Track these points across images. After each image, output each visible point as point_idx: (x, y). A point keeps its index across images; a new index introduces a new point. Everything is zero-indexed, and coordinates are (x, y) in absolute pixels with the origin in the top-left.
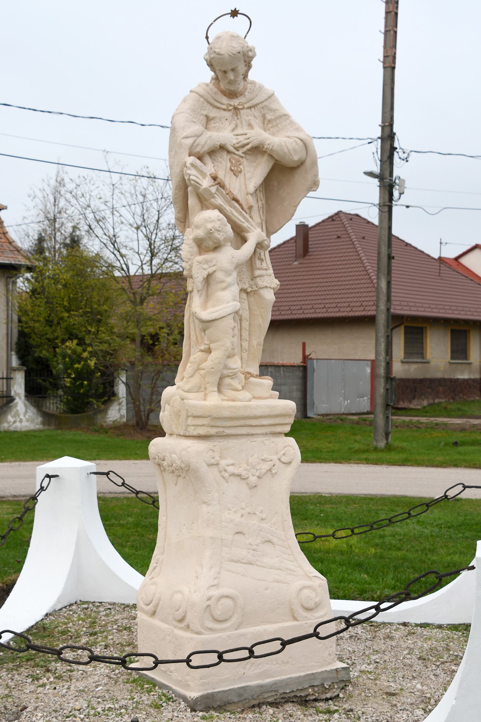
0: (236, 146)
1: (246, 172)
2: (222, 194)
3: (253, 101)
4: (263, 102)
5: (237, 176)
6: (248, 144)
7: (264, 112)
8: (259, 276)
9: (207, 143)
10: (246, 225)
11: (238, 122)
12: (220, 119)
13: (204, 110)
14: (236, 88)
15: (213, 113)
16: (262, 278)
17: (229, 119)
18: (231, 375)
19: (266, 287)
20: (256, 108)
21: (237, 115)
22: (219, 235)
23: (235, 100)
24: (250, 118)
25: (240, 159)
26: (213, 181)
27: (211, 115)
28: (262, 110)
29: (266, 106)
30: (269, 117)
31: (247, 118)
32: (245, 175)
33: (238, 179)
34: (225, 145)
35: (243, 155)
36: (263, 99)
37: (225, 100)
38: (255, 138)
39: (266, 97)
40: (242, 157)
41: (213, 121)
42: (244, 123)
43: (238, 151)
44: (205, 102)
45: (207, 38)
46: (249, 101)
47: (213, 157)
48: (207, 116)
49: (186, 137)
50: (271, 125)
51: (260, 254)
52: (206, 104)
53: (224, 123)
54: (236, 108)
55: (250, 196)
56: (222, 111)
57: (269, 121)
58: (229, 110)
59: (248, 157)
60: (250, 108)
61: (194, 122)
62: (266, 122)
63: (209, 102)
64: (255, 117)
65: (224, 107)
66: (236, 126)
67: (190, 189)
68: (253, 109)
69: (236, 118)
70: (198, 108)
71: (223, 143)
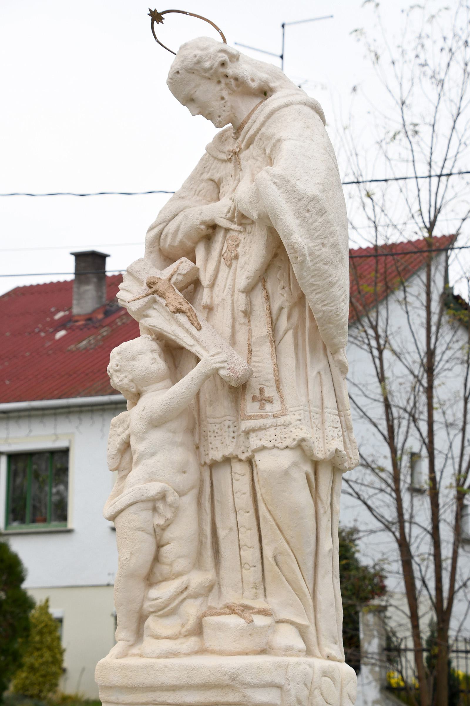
8: (254, 430)
9: (181, 226)
10: (196, 349)
16: (261, 434)
18: (152, 610)
19: (263, 448)
22: (118, 377)
27: (216, 177)
44: (211, 158)
51: (261, 390)
61: (183, 198)
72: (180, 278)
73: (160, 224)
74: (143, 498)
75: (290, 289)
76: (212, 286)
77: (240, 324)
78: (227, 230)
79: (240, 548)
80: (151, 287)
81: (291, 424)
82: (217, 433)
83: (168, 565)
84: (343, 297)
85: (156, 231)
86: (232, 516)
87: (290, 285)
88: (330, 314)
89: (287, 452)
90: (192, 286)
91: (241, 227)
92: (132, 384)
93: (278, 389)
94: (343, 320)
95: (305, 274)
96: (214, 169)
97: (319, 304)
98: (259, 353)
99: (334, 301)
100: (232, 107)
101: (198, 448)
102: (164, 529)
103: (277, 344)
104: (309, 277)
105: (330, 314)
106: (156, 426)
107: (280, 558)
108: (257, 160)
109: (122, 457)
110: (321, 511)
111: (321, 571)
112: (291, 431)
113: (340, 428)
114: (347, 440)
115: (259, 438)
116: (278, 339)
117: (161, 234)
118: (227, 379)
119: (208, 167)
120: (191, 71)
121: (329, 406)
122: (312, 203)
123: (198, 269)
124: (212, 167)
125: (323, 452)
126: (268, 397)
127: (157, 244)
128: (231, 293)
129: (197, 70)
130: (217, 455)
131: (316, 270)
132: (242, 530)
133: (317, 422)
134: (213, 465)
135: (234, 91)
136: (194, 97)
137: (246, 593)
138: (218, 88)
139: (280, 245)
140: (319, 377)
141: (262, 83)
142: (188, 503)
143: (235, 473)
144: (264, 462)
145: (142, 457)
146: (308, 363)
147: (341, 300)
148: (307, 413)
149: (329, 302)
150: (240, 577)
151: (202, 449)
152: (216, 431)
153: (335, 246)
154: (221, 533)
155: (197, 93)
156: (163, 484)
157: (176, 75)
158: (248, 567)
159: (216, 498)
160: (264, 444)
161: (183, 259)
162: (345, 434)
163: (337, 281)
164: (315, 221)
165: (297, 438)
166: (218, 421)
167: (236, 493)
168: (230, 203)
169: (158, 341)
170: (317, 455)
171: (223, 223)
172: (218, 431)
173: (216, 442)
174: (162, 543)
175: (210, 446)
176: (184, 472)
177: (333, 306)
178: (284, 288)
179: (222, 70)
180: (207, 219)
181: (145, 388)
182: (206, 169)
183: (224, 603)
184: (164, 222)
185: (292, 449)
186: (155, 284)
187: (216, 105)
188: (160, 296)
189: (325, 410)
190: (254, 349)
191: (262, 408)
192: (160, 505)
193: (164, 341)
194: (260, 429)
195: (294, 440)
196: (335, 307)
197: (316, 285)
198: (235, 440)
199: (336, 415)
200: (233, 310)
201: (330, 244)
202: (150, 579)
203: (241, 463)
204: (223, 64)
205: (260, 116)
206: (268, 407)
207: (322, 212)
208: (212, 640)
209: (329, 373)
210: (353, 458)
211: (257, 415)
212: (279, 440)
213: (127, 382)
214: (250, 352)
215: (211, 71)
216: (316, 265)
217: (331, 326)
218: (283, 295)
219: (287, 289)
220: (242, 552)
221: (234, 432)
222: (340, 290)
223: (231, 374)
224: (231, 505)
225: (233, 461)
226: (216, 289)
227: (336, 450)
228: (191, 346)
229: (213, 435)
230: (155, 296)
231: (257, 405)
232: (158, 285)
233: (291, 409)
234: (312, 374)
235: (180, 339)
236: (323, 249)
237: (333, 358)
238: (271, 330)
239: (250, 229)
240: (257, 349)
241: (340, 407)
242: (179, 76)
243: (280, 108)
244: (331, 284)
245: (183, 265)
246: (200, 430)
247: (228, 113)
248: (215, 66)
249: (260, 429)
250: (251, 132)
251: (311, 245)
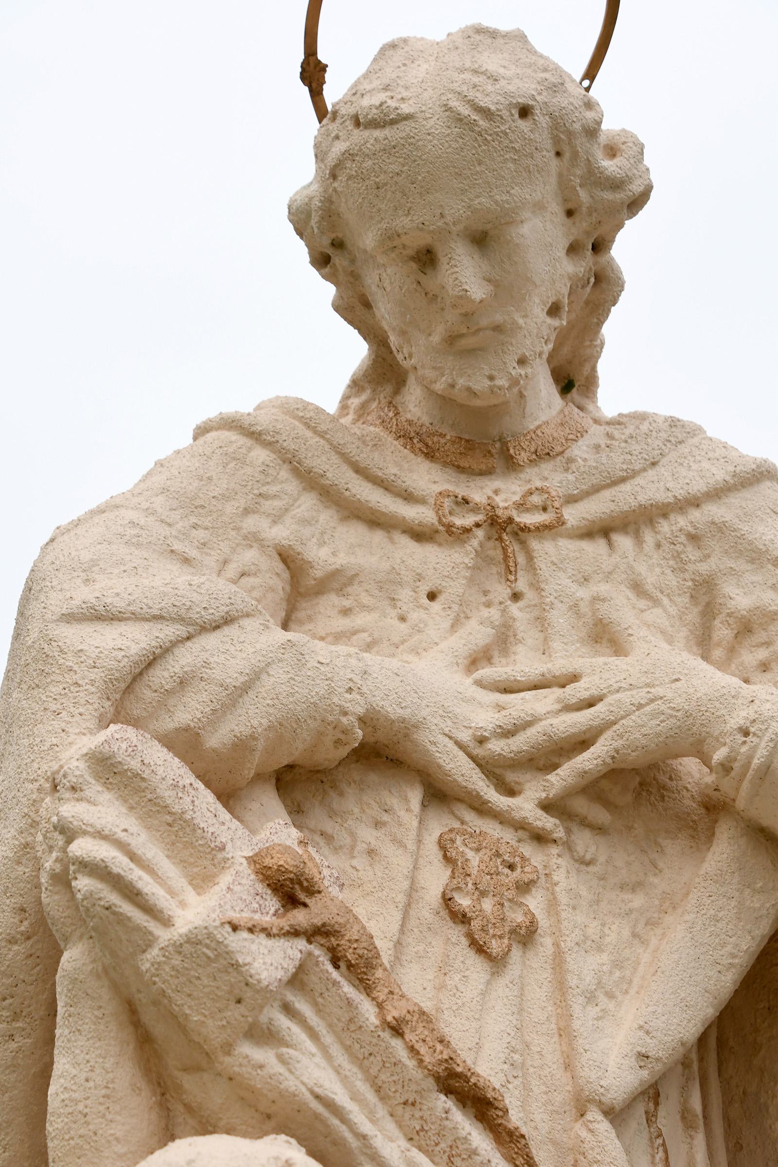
0: (497, 746)
1: (568, 943)
2: (350, 1025)
3: (626, 487)
4: (694, 502)
5: (498, 963)
6: (582, 743)
7: (703, 568)
9: (267, 682)
11: (514, 609)
12: (388, 586)
13: (276, 519)
14: (501, 382)
15: (335, 546)
17: (454, 588)
20: (649, 538)
21: (509, 571)
23: (496, 483)
24: (603, 588)
25: (527, 849)
26: (272, 903)
28: (692, 553)
29: (720, 528)
30: (740, 596)
31: (583, 593)
32: (558, 961)
33: (503, 988)
34: (407, 729)
35: (547, 822)
36: (698, 486)
37: (427, 478)
38: (640, 696)
39: (719, 474)
40: (540, 838)
41: (330, 602)
42: (560, 618)
43: (511, 792)
44: (284, 473)
45: (313, 73)
46: (596, 489)
47: (318, 818)
48: (289, 559)
49: (101, 616)
50: (762, 654)
52: (292, 486)
53: (415, 616)
54: (499, 526)
55: (603, 1126)
56: (405, 541)
57: (745, 628)
58: (449, 528)
59: (584, 841)
60: (602, 531)
62: (722, 632)
63: (312, 481)
64: (638, 588)
65: (420, 514)
66: (504, 640)
67: (73, 958)
68: (624, 542)
69: (501, 591)
70: (225, 498)
71: (392, 710)
73: (158, 618)
96: (305, 522)
108: (656, 602)
119: (277, 503)
129: (575, 155)
182: (267, 505)
184: (181, 620)
188: (335, 962)
215: (608, 196)
242: (524, 125)
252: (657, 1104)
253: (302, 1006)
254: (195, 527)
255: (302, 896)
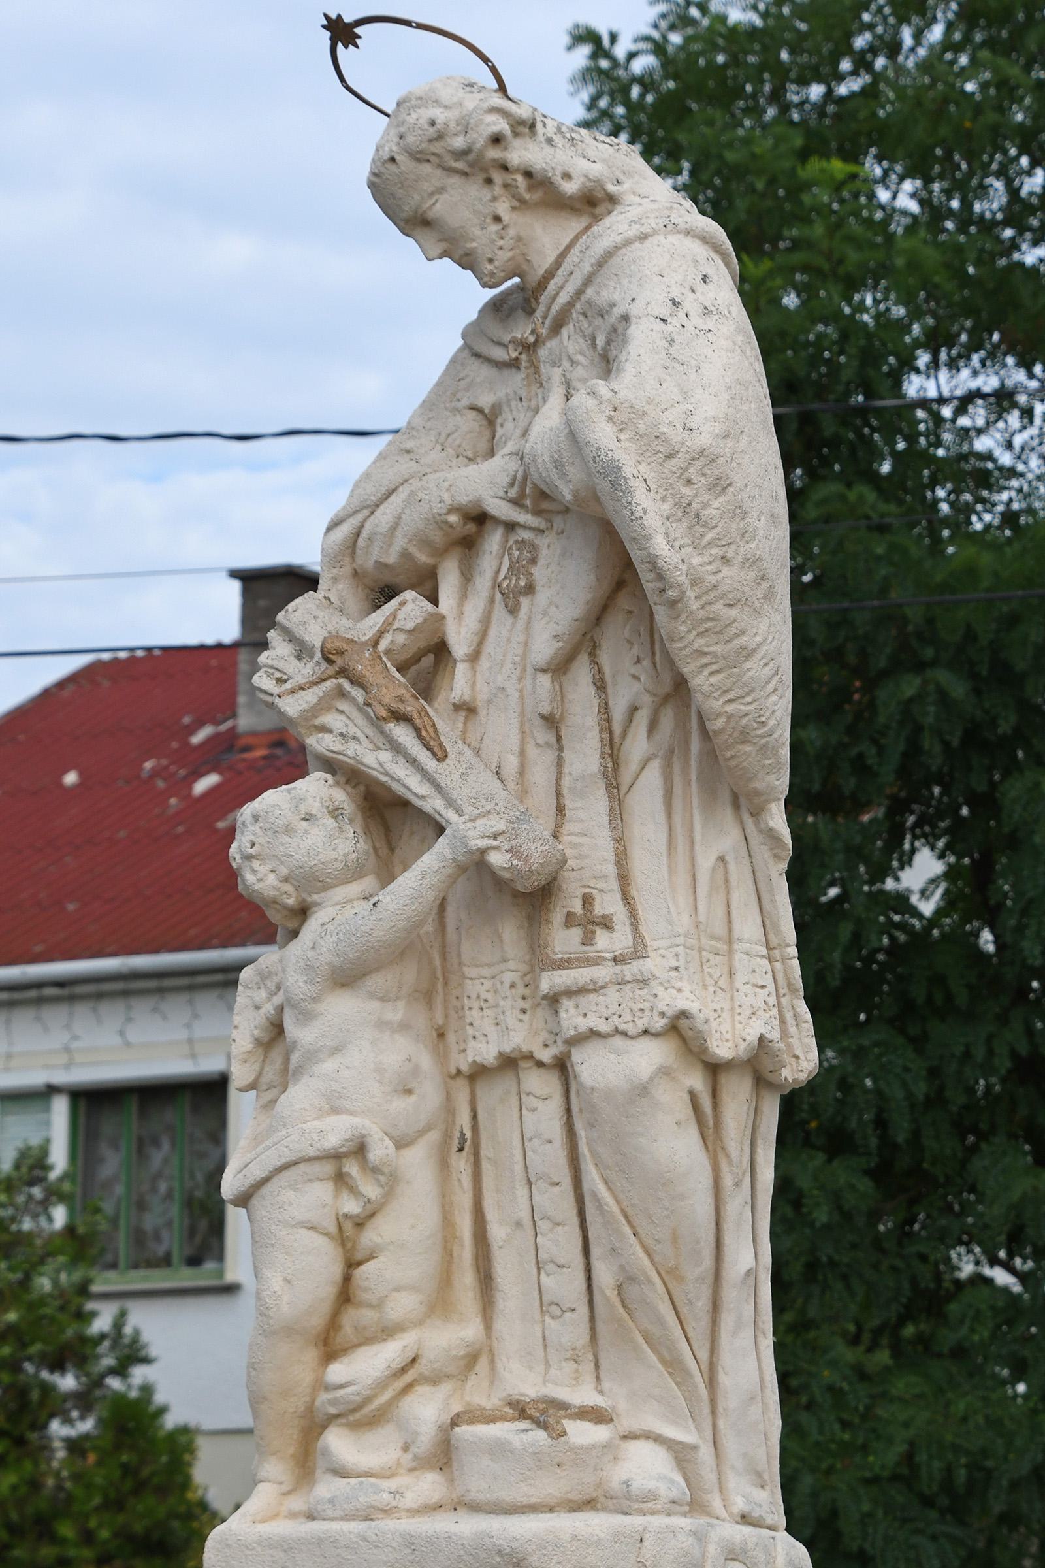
10: (433, 804)
18: (333, 1410)
19: (593, 1034)
22: (254, 871)
27: (486, 400)
51: (587, 900)
72: (401, 638)
73: (356, 512)
74: (312, 1153)
75: (654, 664)
76: (474, 657)
77: (538, 745)
78: (511, 526)
79: (539, 1269)
80: (330, 662)
81: (655, 977)
82: (486, 1000)
83: (370, 1306)
84: (774, 682)
85: (346, 529)
86: (522, 1192)
87: (653, 654)
88: (744, 721)
89: (646, 1044)
90: (430, 659)
91: (540, 520)
92: (288, 888)
93: (627, 898)
94: (775, 736)
95: (683, 628)
97: (716, 699)
98: (582, 815)
99: (752, 691)
100: (519, 239)
101: (441, 1035)
102: (360, 1223)
103: (622, 793)
104: (691, 637)
105: (744, 721)
106: (343, 985)
107: (633, 1291)
109: (266, 1057)
110: (728, 1181)
111: (727, 1321)
112: (656, 995)
113: (771, 988)
114: (789, 1016)
115: (581, 1011)
116: (626, 778)
117: (358, 535)
118: (506, 875)
119: (468, 380)
120: (419, 157)
121: (746, 936)
122: (698, 465)
123: (444, 617)
124: (478, 379)
125: (730, 1044)
126: (604, 917)
127: (347, 559)
128: (518, 672)
130: (486, 1051)
131: (709, 619)
132: (543, 1225)
133: (716, 973)
134: (478, 1074)
135: (522, 201)
136: (431, 215)
137: (553, 1372)
138: (486, 194)
139: (628, 564)
140: (721, 869)
141: (588, 184)
142: (417, 1164)
143: (528, 1094)
144: (596, 1067)
145: (312, 1056)
146: (698, 837)
147: (770, 687)
148: (695, 953)
149: (740, 692)
150: (540, 1335)
151: (451, 1038)
152: (484, 995)
153: (754, 562)
154: (497, 1232)
155: (438, 205)
156: (357, 1121)
157: (390, 166)
158: (559, 1313)
159: (484, 1153)
160: (592, 1025)
161: (409, 595)
162: (784, 1001)
163: (759, 645)
164: (706, 505)
165: (670, 1012)
166: (486, 972)
167: (531, 1140)
168: (514, 465)
169: (349, 789)
170: (717, 1051)
171: (500, 509)
172: (489, 996)
173: (481, 1020)
174: (358, 1256)
175: (470, 1030)
176: (409, 1092)
177: (749, 703)
178: (638, 661)
179: (493, 153)
180: (463, 499)
181: (316, 897)
183: (504, 1394)
185: (656, 1035)
186: (341, 653)
187: (482, 238)
189: (736, 946)
190: (568, 802)
191: (588, 939)
192: (352, 1168)
193: (362, 788)
194: (582, 991)
195: (662, 1014)
196: (754, 705)
197: (709, 653)
198: (526, 1017)
199: (762, 957)
200: (522, 714)
201: (740, 558)
202: (330, 1346)
203: (542, 1070)
204: (497, 140)
205: (580, 263)
206: (602, 940)
207: (720, 485)
208: (478, 1479)
209: (746, 861)
210: (802, 1057)
211: (577, 959)
212: (628, 1017)
213: (276, 883)
214: (560, 810)
216: (708, 608)
217: (748, 748)
218: (636, 677)
219: (646, 663)
220: (543, 1275)
221: (524, 998)
222: (766, 665)
223: (515, 862)
224: (519, 1167)
225: (523, 1064)
226: (484, 663)
227: (762, 1038)
228: (423, 797)
229: (476, 1005)
230: (341, 681)
231: (576, 934)
232: (346, 656)
233: (656, 944)
234: (706, 862)
235: (399, 781)
236: (726, 572)
237: (757, 824)
238: (609, 760)
239: (562, 525)
240: (579, 804)
241: (771, 937)
242: (392, 167)
243: (628, 242)
244: (747, 653)
245: (410, 608)
246: (445, 995)
247: (510, 254)
248: (478, 146)
249: (582, 991)
250: (563, 298)
251: (696, 561)
252: (594, 647)
253: (343, 705)
254: (429, 419)
255: (333, 657)
